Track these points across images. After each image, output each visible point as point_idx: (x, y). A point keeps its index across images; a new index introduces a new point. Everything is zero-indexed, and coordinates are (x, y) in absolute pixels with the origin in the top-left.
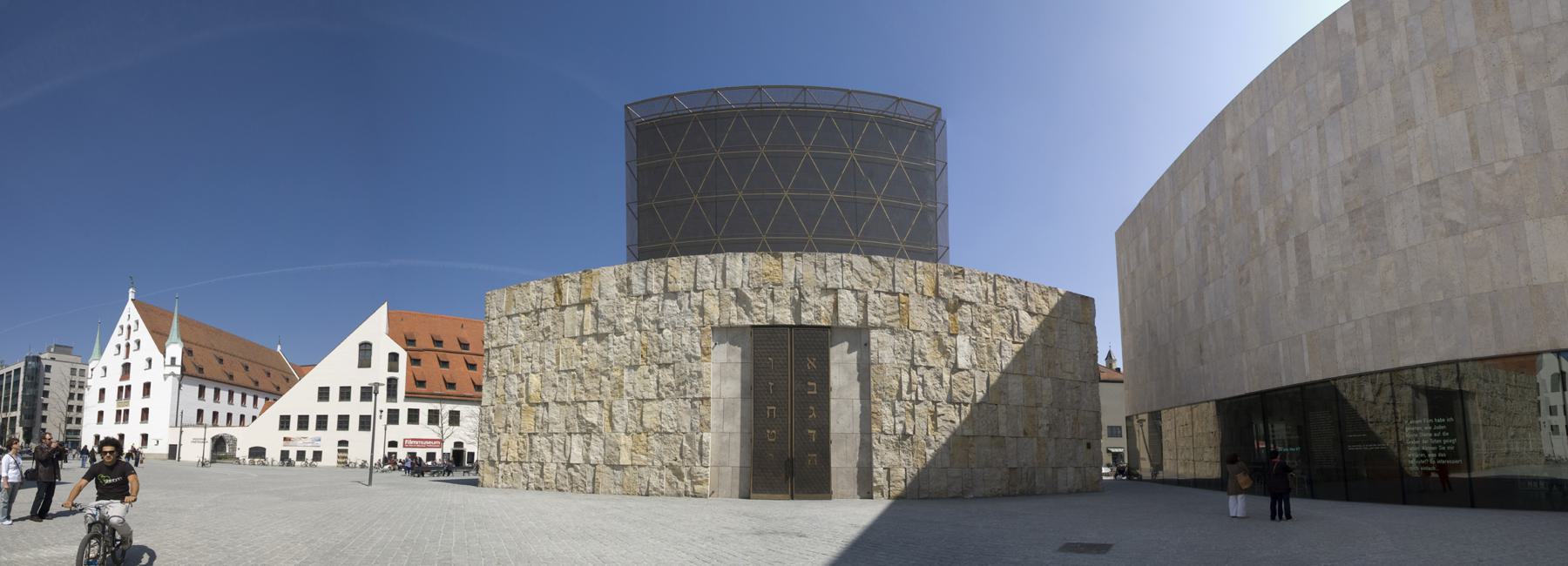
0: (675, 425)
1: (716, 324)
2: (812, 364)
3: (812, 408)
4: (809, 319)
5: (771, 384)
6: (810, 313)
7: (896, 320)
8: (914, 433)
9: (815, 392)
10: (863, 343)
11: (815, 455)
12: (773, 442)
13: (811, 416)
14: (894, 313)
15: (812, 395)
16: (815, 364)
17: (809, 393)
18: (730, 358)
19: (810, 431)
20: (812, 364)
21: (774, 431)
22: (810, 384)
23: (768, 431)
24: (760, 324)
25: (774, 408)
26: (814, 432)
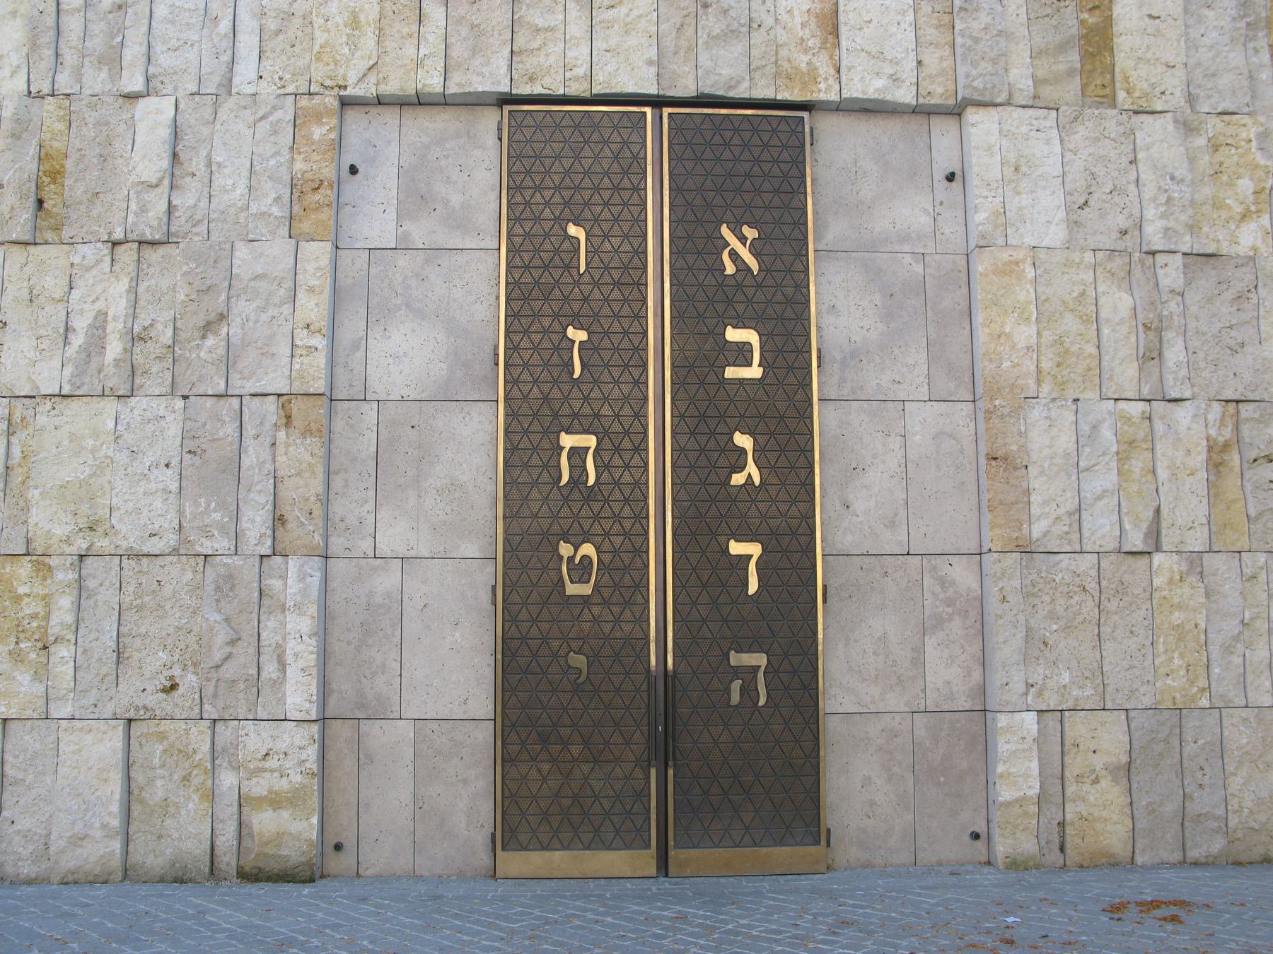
0: (171, 520)
1: (367, 89)
2: (734, 243)
3: (743, 441)
4: (726, 72)
5: (580, 336)
6: (738, 48)
7: (1070, 73)
8: (1158, 548)
9: (755, 372)
10: (945, 159)
11: (760, 660)
12: (584, 600)
13: (738, 479)
14: (1062, 48)
15: (741, 382)
16: (756, 254)
17: (731, 372)
18: (408, 226)
19: (736, 548)
20: (734, 243)
21: (588, 549)
22: (733, 335)
23: (565, 550)
24: (537, 90)
25: (591, 441)
26: (754, 549)
